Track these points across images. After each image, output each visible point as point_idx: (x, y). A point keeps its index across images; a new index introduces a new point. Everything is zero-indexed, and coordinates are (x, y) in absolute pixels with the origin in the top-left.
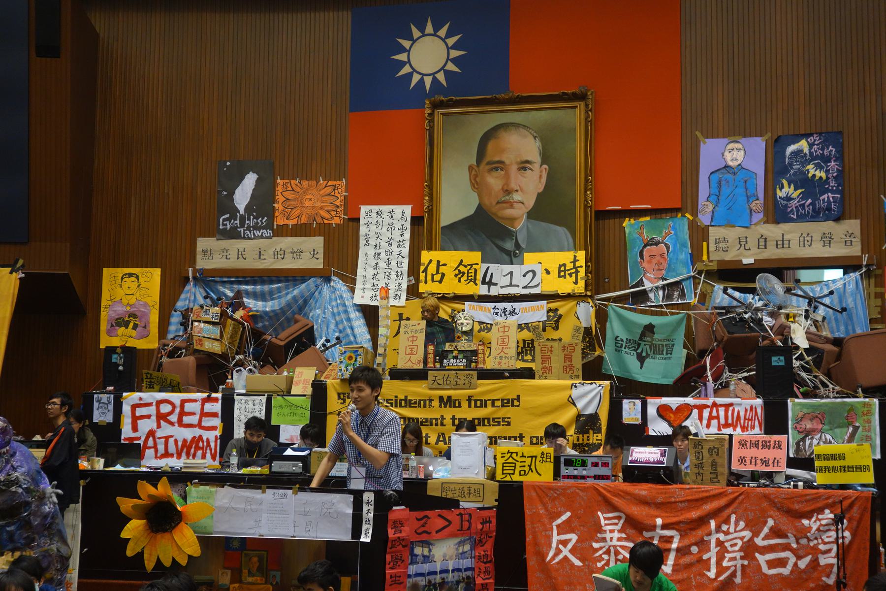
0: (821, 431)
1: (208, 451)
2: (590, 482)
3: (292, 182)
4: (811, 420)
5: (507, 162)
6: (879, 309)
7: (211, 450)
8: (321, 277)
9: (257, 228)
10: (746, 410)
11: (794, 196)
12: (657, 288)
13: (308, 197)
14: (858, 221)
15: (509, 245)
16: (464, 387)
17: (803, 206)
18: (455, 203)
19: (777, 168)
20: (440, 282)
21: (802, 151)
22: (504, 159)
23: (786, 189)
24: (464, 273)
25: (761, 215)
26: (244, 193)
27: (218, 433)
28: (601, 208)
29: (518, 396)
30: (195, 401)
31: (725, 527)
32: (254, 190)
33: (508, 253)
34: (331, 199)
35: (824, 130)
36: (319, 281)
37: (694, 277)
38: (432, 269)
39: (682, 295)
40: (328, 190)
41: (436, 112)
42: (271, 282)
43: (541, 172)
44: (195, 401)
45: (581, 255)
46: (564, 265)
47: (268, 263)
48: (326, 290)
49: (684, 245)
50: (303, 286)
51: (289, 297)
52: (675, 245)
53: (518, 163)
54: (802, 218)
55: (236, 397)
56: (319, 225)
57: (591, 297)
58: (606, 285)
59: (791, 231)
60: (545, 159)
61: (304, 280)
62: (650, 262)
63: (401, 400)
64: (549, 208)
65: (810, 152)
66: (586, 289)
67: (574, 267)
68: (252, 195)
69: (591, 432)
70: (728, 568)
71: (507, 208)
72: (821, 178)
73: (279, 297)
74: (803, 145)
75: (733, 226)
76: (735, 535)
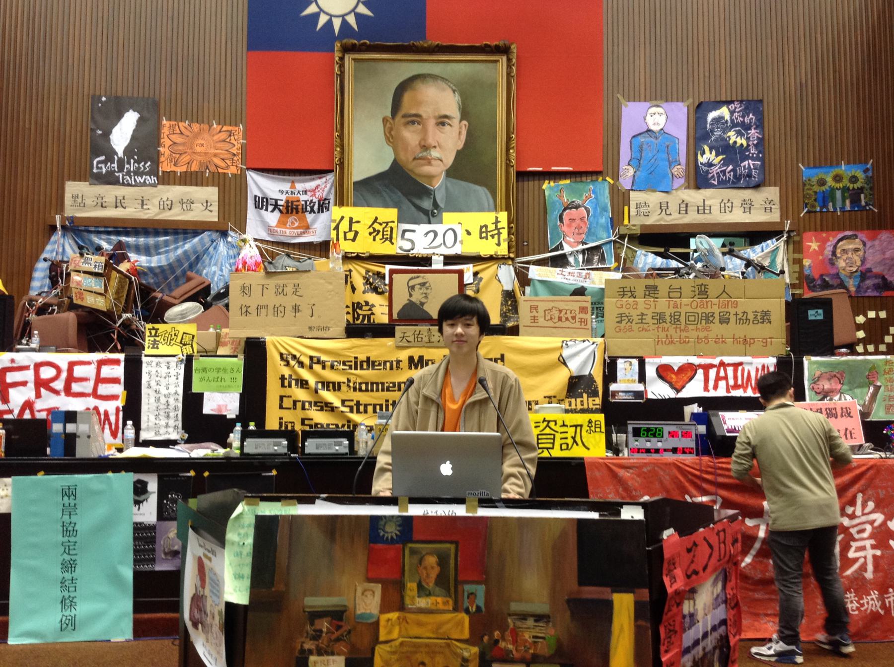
0: (841, 392)
1: (107, 426)
2: (670, 457)
3: (181, 124)
4: (829, 380)
5: (424, 115)
6: (797, 275)
7: (110, 424)
8: (217, 231)
9: (138, 173)
10: (757, 370)
11: (716, 161)
12: (577, 251)
13: (200, 141)
14: (778, 188)
15: (427, 204)
16: (439, 344)
17: (724, 172)
18: (368, 157)
19: (699, 135)
20: (354, 240)
21: (723, 118)
22: (421, 112)
23: (707, 155)
24: (379, 232)
25: (682, 181)
27: (120, 403)
28: (522, 169)
29: (503, 356)
30: (89, 363)
31: (849, 510)
32: (134, 131)
33: (425, 212)
34: (227, 146)
35: (745, 98)
36: (215, 235)
37: (615, 242)
38: (344, 226)
39: (602, 259)
40: (223, 136)
41: (347, 57)
42: (157, 233)
43: (461, 128)
44: (89, 363)
45: (503, 216)
46: (486, 226)
47: (152, 212)
48: (222, 247)
49: (604, 209)
50: (196, 240)
51: (180, 251)
52: (595, 209)
53: (435, 117)
54: (723, 184)
55: (144, 359)
56: (213, 174)
57: (512, 259)
58: (525, 248)
59: (712, 197)
60: (465, 115)
61: (196, 233)
62: (569, 226)
63: (362, 362)
64: (469, 167)
65: (732, 121)
66: (509, 252)
67: (496, 228)
68: (133, 138)
69: (585, 395)
70: (855, 560)
71: (425, 165)
72: (742, 145)
73: (167, 252)
74: (724, 112)
75: (655, 191)
76: (864, 519)
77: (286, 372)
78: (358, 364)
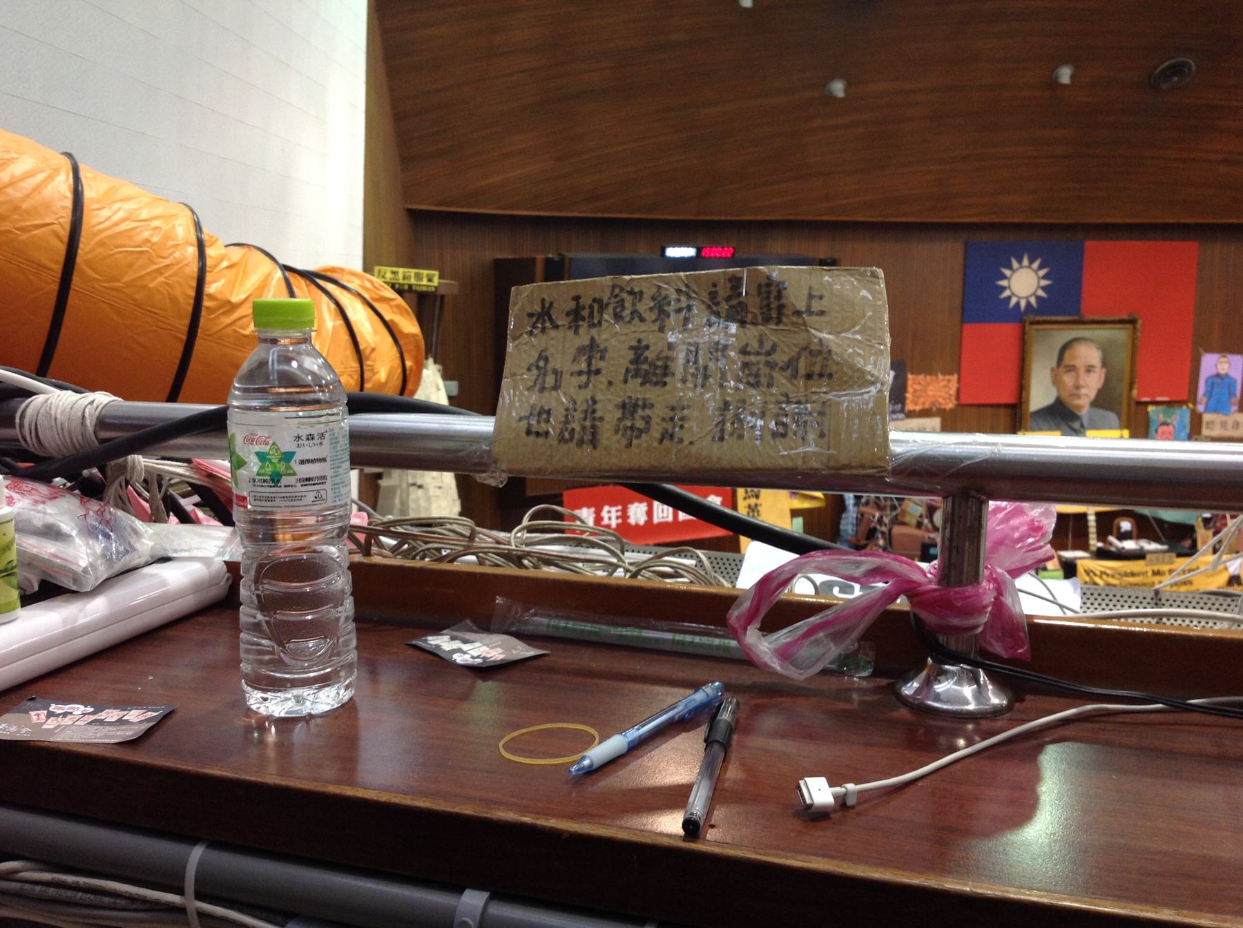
15: (1076, 425)
40: (944, 383)
60: (1105, 363)
64: (1103, 400)
77: (1087, 579)
78: (1126, 575)
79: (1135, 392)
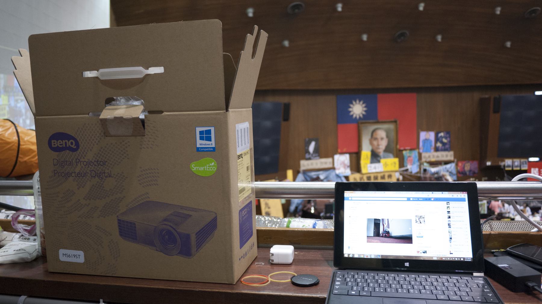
9: (316, 156)
15: (379, 159)
19: (437, 139)
26: (312, 148)
47: (319, 166)
59: (439, 154)
60: (387, 136)
64: (387, 150)
79: (398, 147)
